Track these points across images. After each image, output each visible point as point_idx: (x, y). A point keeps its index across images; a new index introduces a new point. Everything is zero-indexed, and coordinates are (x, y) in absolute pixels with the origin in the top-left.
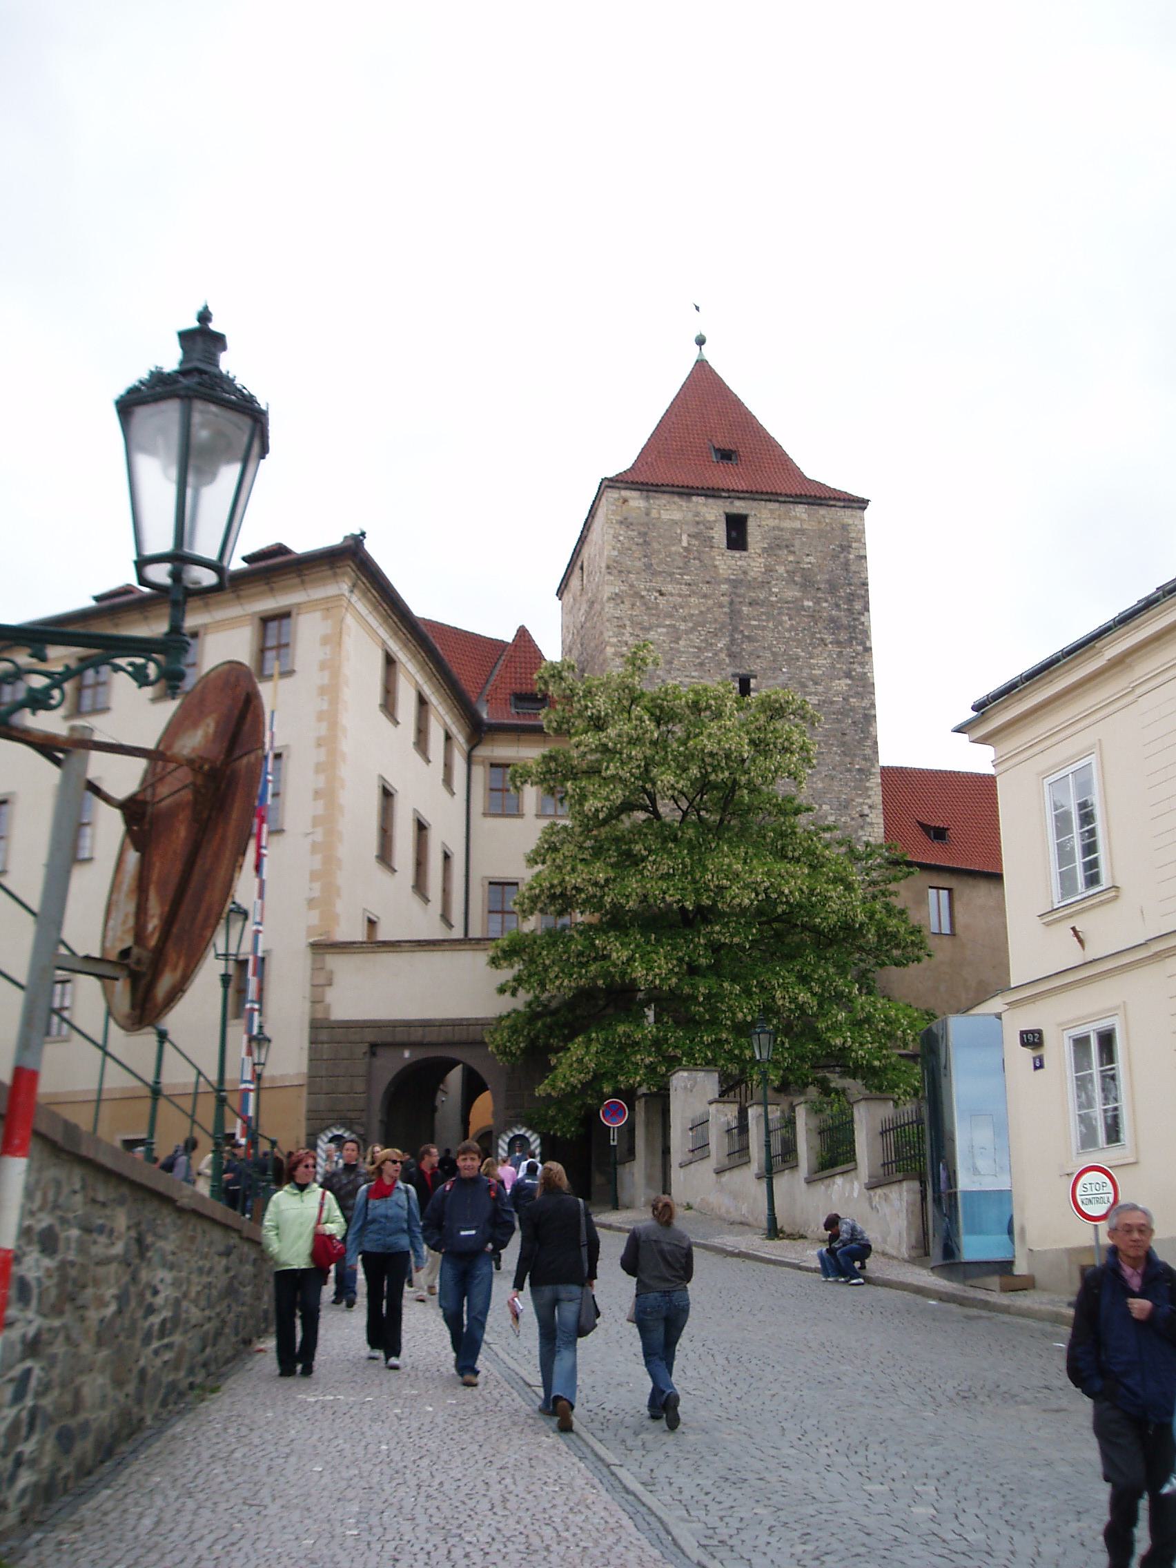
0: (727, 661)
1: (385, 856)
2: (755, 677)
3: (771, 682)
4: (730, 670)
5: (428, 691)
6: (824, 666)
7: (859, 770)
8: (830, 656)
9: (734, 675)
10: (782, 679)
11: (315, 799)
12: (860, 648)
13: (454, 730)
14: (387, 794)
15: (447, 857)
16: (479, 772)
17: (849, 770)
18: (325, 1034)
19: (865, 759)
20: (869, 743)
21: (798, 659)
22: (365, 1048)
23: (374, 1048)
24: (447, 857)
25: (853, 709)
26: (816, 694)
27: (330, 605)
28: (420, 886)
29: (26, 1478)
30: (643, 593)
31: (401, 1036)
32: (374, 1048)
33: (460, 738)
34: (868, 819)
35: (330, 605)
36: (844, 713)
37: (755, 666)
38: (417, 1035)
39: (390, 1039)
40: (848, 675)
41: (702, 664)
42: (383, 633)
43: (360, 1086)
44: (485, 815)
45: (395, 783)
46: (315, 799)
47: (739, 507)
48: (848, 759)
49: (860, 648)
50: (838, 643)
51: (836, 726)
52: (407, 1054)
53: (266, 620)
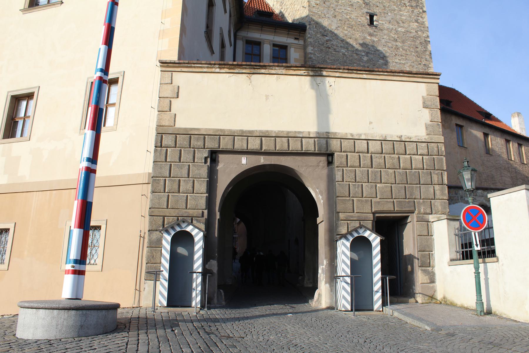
0: (364, 5)
2: (376, 15)
3: (384, 19)
4: (366, 10)
6: (405, 16)
7: (424, 65)
8: (408, 12)
9: (367, 13)
10: (389, 18)
12: (421, 11)
16: (240, 44)
17: (420, 64)
18: (170, 141)
19: (426, 60)
20: (428, 53)
21: (394, 10)
23: (213, 156)
25: (419, 37)
26: (403, 27)
31: (240, 144)
36: (415, 38)
37: (376, 10)
38: (254, 144)
39: (230, 147)
40: (417, 21)
41: (352, 5)
43: (202, 187)
48: (419, 59)
49: (421, 11)
50: (412, 6)
51: (413, 43)
52: (244, 160)
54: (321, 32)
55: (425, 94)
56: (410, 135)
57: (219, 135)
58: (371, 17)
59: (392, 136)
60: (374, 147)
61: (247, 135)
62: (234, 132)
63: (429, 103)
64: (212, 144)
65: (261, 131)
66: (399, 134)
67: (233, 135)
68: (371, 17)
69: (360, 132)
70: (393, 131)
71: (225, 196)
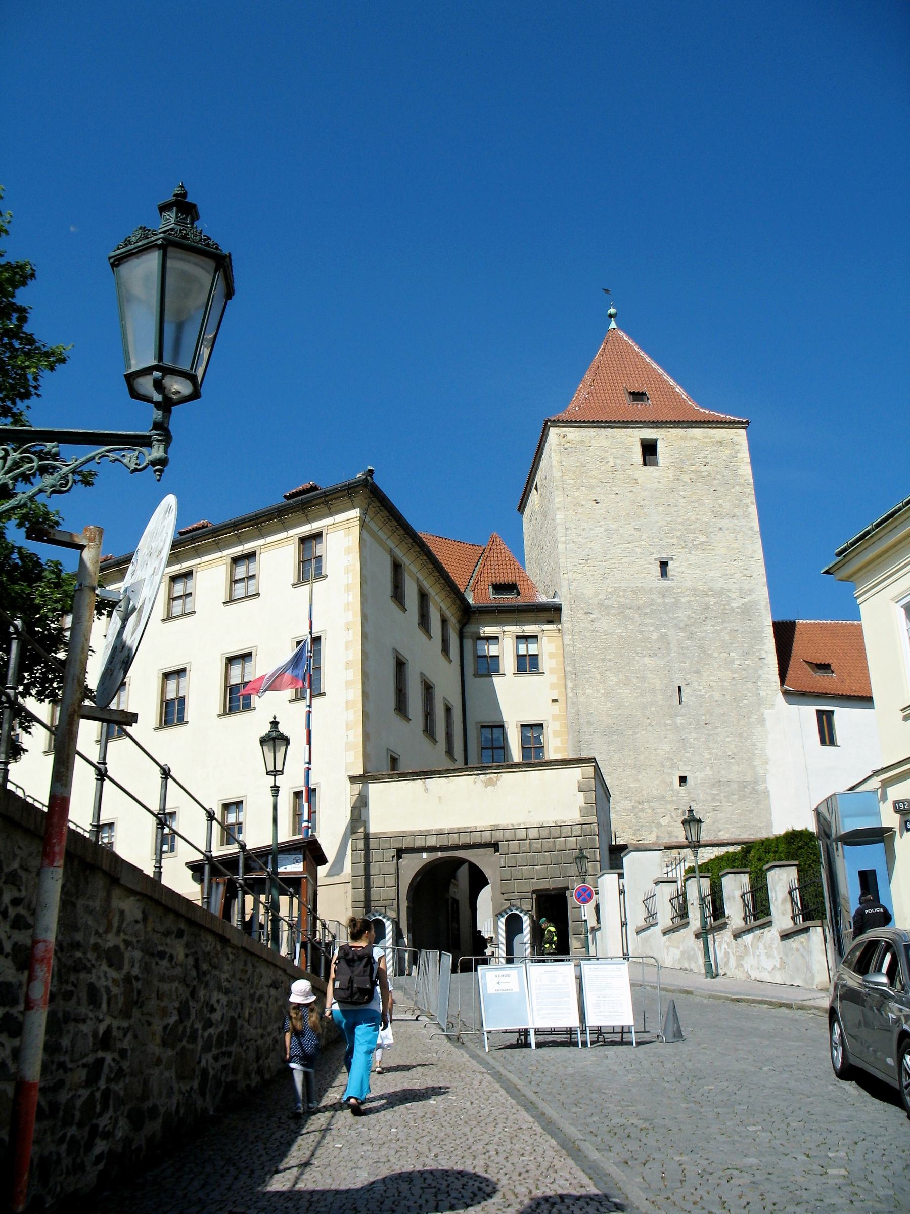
1: (401, 707)
5: (426, 584)
11: (347, 669)
13: (448, 614)
14: (400, 665)
15: (448, 710)
22: (393, 852)
24: (448, 710)
27: (351, 525)
28: (429, 730)
29: (101, 1146)
30: (583, 503)
31: (420, 843)
32: (400, 853)
33: (453, 621)
34: (765, 661)
35: (351, 525)
38: (432, 841)
42: (391, 544)
43: (391, 881)
44: (477, 675)
45: (406, 654)
46: (347, 669)
47: (649, 434)
52: (425, 855)
53: (303, 540)
54: (582, 608)
55: (580, 778)
56: (565, 819)
57: (403, 835)
58: (664, 565)
59: (548, 822)
60: (533, 833)
61: (425, 834)
62: (414, 832)
63: (584, 787)
64: (399, 846)
65: (436, 830)
66: (554, 820)
67: (414, 835)
68: (664, 565)
69: (520, 822)
70: (550, 817)
71: (415, 884)
